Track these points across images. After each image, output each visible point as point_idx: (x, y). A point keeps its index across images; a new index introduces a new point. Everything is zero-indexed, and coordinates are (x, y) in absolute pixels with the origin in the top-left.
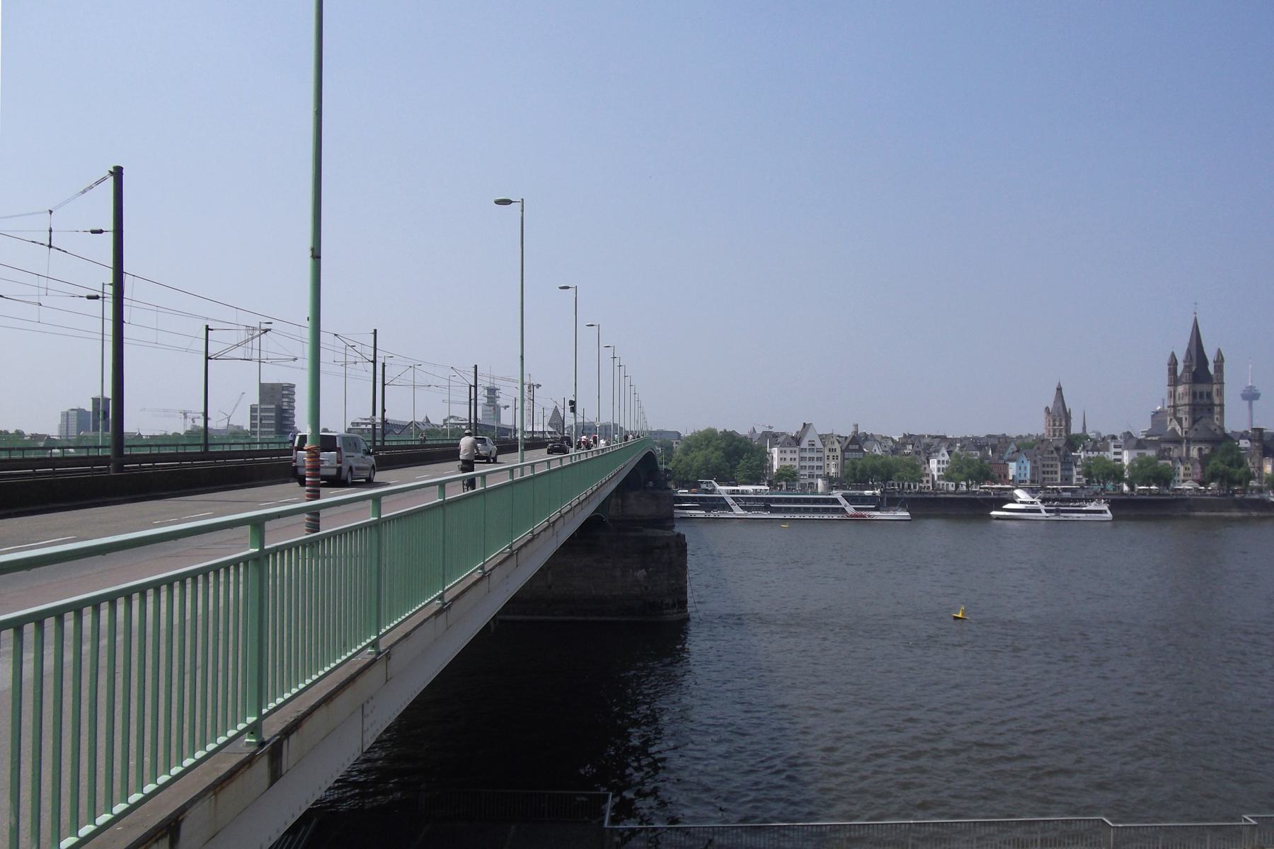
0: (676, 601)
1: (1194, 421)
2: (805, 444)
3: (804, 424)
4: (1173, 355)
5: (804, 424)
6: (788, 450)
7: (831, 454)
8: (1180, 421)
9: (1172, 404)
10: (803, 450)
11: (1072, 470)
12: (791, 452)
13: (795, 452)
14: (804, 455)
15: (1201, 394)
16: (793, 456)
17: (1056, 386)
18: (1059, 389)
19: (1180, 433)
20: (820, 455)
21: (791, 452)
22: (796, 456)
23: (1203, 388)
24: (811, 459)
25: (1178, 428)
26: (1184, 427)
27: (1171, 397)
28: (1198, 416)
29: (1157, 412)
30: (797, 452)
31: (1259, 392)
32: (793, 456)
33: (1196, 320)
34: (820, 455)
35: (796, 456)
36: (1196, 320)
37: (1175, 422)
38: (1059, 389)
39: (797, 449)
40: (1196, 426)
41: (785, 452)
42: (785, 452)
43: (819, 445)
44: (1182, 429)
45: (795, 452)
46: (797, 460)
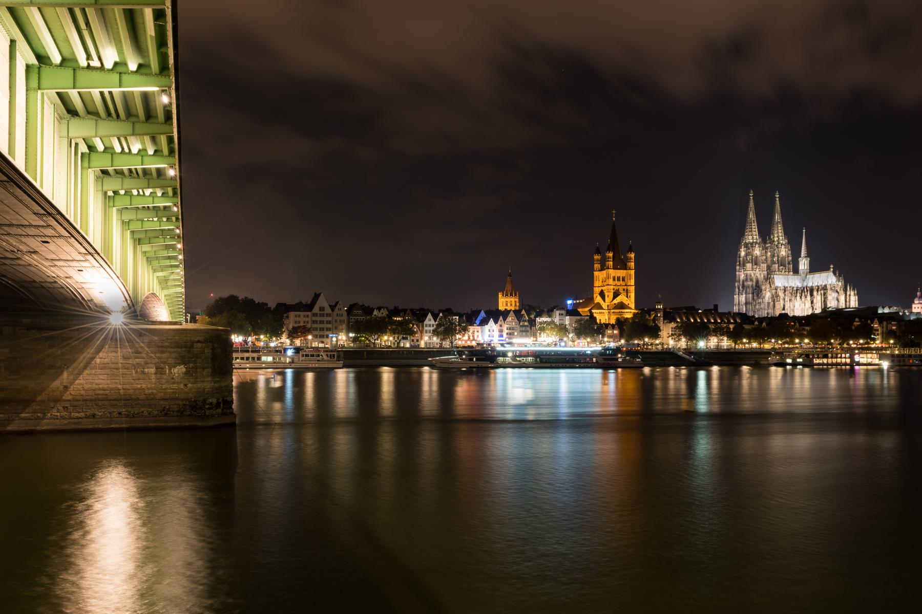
0: (221, 400)
2: (316, 309)
3: (315, 293)
5: (315, 293)
6: (302, 314)
7: (339, 318)
10: (315, 315)
12: (304, 316)
13: (308, 316)
14: (315, 318)
16: (306, 319)
20: (329, 319)
21: (304, 316)
22: (309, 319)
24: (322, 322)
30: (310, 316)
32: (306, 319)
34: (329, 319)
35: (309, 319)
39: (309, 313)
41: (299, 316)
42: (299, 316)
43: (328, 310)
45: (308, 316)
46: (310, 322)
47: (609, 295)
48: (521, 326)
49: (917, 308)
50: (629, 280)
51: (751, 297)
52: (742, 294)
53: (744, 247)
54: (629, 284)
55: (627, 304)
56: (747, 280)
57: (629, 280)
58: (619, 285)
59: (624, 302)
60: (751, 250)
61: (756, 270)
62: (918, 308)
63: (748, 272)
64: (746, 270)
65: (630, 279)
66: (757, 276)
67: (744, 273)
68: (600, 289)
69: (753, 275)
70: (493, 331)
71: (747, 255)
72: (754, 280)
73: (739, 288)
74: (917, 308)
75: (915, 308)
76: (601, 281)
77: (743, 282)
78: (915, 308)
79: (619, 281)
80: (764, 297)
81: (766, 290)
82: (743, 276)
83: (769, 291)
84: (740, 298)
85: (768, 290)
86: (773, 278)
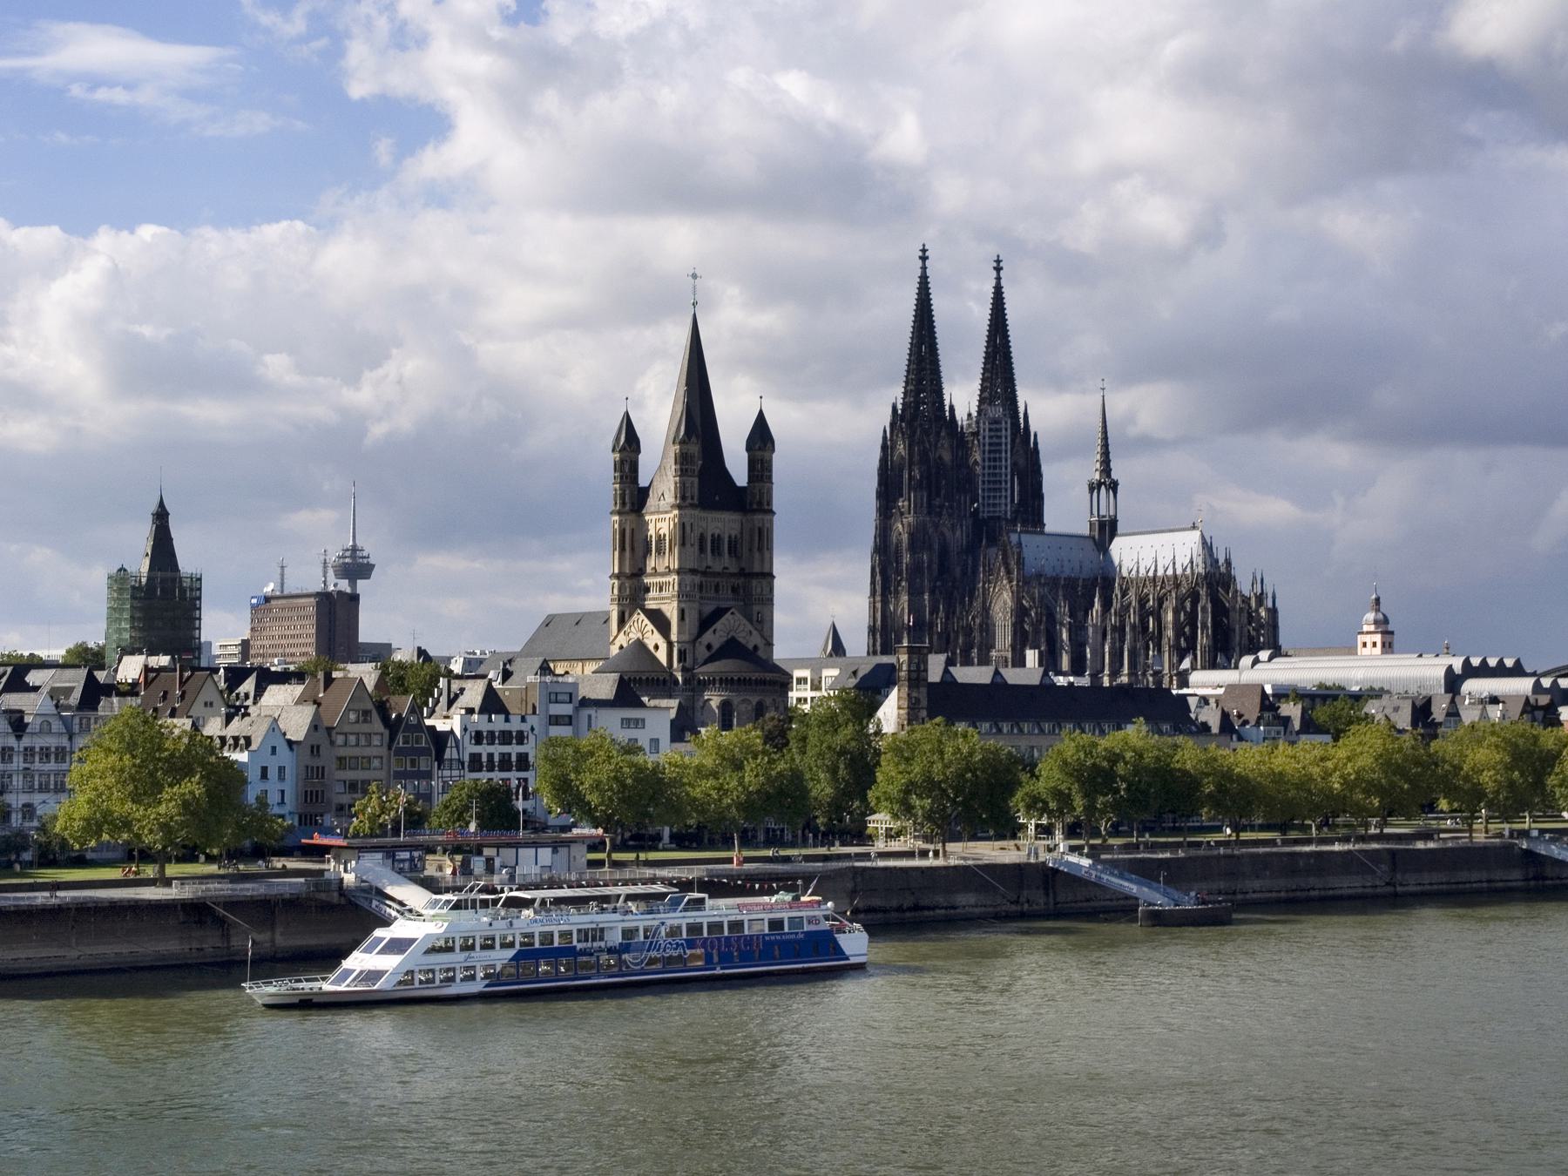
1: (706, 623)
4: (628, 426)
8: (659, 620)
9: (616, 571)
11: (428, 775)
15: (717, 541)
17: (154, 507)
19: (662, 656)
23: (724, 523)
25: (653, 639)
26: (674, 637)
27: (622, 549)
28: (709, 609)
29: (267, 599)
31: (372, 561)
33: (695, 315)
36: (695, 315)
37: (640, 619)
40: (708, 637)
44: (670, 645)
48: (399, 752)
49: (1369, 645)
50: (757, 555)
54: (757, 569)
55: (750, 647)
57: (757, 555)
58: (718, 568)
59: (741, 640)
61: (940, 515)
62: (1374, 644)
65: (760, 549)
66: (942, 534)
69: (931, 530)
70: (264, 770)
72: (936, 547)
74: (1369, 645)
75: (1365, 645)
78: (1365, 645)
79: (720, 554)
86: (1020, 544)
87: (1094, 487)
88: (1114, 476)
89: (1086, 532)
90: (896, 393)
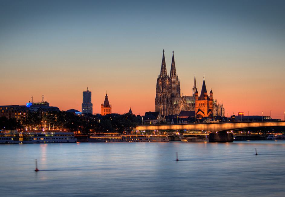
18: (106, 96)
38: (106, 96)
47: (206, 112)
51: (166, 106)
52: (160, 105)
53: (161, 80)
56: (163, 97)
60: (165, 82)
63: (165, 93)
64: (163, 92)
67: (161, 94)
68: (198, 108)
71: (163, 84)
73: (158, 101)
76: (199, 105)
77: (160, 98)
80: (179, 108)
81: (180, 104)
82: (160, 95)
83: (183, 104)
84: (159, 107)
85: (182, 104)
87: (193, 89)
88: (197, 87)
89: (192, 96)
90: (159, 72)
